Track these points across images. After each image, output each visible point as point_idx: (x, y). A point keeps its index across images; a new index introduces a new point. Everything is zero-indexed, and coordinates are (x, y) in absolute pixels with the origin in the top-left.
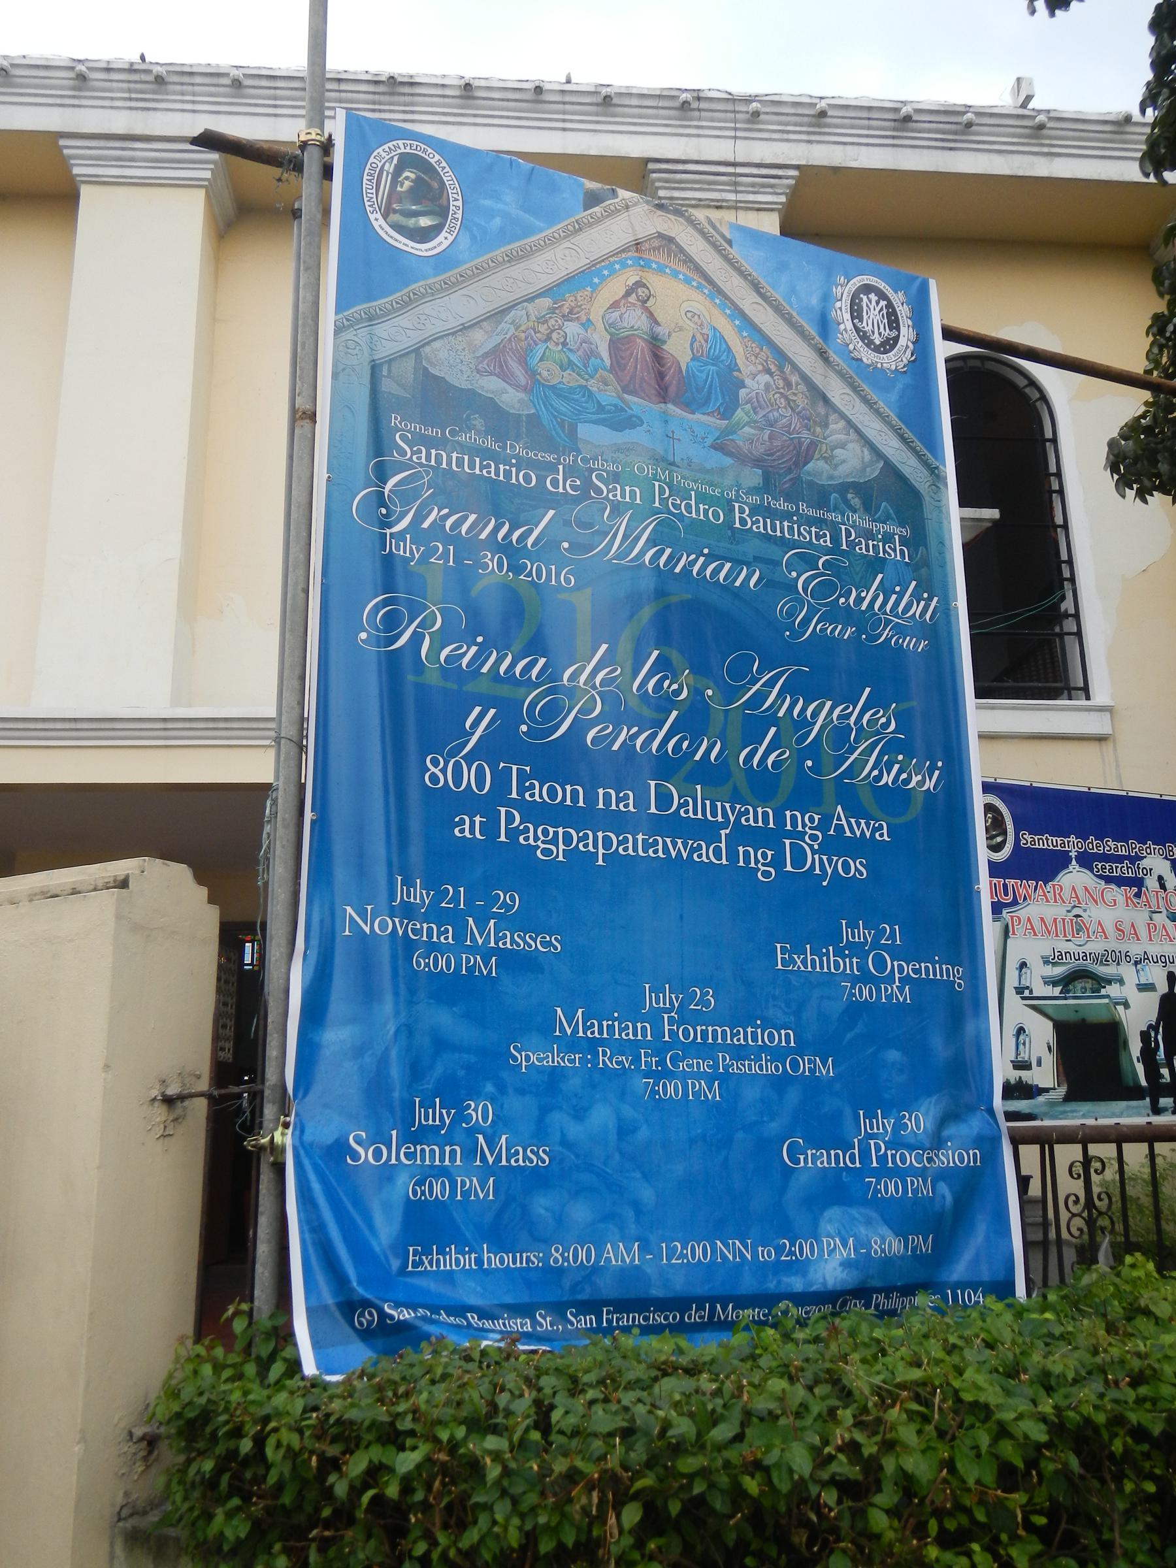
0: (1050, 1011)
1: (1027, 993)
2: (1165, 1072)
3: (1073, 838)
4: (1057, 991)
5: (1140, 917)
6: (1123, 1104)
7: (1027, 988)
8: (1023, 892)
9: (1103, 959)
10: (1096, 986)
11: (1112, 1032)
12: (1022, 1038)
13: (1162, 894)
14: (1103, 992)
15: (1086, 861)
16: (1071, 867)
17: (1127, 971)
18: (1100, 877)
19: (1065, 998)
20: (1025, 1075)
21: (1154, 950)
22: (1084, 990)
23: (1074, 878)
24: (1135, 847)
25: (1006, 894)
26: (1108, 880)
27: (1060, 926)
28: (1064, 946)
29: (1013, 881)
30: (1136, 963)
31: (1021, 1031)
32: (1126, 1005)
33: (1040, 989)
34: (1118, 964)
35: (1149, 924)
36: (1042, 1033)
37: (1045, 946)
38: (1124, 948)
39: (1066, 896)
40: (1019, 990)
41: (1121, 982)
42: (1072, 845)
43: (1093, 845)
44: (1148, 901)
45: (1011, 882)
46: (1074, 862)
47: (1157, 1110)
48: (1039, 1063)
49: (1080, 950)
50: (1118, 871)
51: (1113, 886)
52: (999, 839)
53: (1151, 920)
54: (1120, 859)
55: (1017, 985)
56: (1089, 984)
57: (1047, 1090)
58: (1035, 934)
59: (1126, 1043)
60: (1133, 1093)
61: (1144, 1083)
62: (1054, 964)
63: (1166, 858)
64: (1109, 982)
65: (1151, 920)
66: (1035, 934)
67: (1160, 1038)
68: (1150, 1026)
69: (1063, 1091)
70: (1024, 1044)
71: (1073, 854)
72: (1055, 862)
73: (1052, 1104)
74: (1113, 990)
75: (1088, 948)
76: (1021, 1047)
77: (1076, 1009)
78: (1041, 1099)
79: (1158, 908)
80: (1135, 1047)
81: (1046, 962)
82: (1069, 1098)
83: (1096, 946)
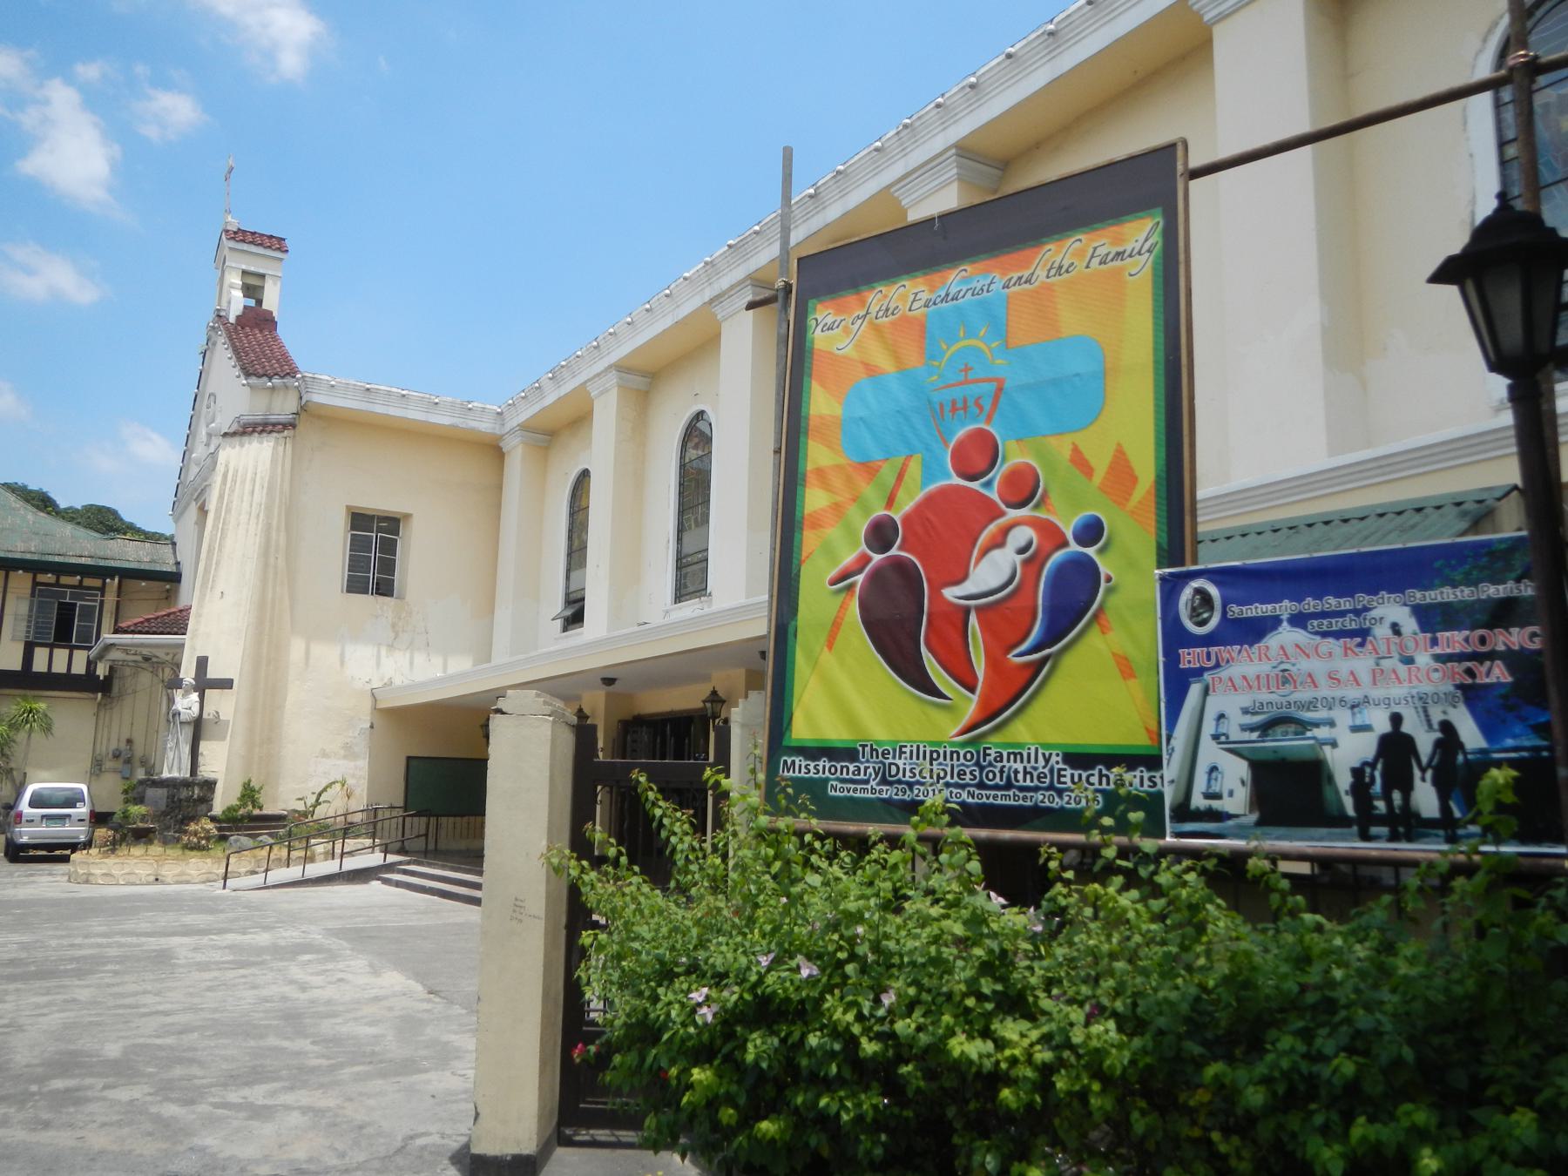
0: (1246, 753)
1: (1223, 739)
2: (1381, 805)
3: (1286, 603)
4: (1255, 736)
5: (1362, 664)
6: (1323, 831)
7: (1224, 734)
8: (1225, 656)
9: (1311, 705)
10: (1300, 729)
11: (1313, 771)
12: (1214, 775)
13: (1396, 639)
14: (1309, 734)
15: (1299, 620)
16: (1280, 629)
17: (1344, 718)
18: (1316, 633)
19: (1263, 741)
20: (1216, 804)
21: (1376, 693)
22: (1286, 733)
23: (1287, 636)
24: (1363, 599)
25: (1209, 659)
26: (1325, 635)
27: (1263, 681)
28: (1264, 696)
29: (1216, 649)
30: (1353, 707)
31: (1214, 769)
32: (1334, 744)
33: (1236, 734)
34: (1330, 709)
35: (1374, 670)
36: (1236, 772)
37: (1245, 700)
38: (1338, 693)
39: (1272, 653)
40: (1216, 737)
41: (1332, 724)
42: (1286, 608)
43: (1310, 604)
44: (1375, 649)
45: (1213, 650)
46: (1285, 624)
47: (1365, 836)
48: (1231, 794)
49: (1284, 700)
50: (1337, 624)
51: (1331, 640)
52: (1205, 615)
53: (1378, 665)
54: (1342, 614)
55: (1213, 732)
56: (1292, 728)
57: (1237, 816)
58: (1236, 690)
59: (1330, 779)
60: (1340, 820)
61: (1350, 810)
62: (1256, 713)
63: (1405, 605)
64: (1317, 725)
65: (1378, 665)
66: (1236, 690)
67: (1377, 774)
68: (1365, 764)
69: (1254, 817)
70: (1216, 779)
71: (1285, 617)
72: (1264, 627)
73: (1241, 827)
74: (1322, 733)
75: (1293, 698)
76: (1213, 782)
77: (1275, 750)
78: (1230, 823)
79: (1389, 652)
80: (1344, 781)
81: (1246, 711)
82: (1260, 823)
83: (1304, 695)
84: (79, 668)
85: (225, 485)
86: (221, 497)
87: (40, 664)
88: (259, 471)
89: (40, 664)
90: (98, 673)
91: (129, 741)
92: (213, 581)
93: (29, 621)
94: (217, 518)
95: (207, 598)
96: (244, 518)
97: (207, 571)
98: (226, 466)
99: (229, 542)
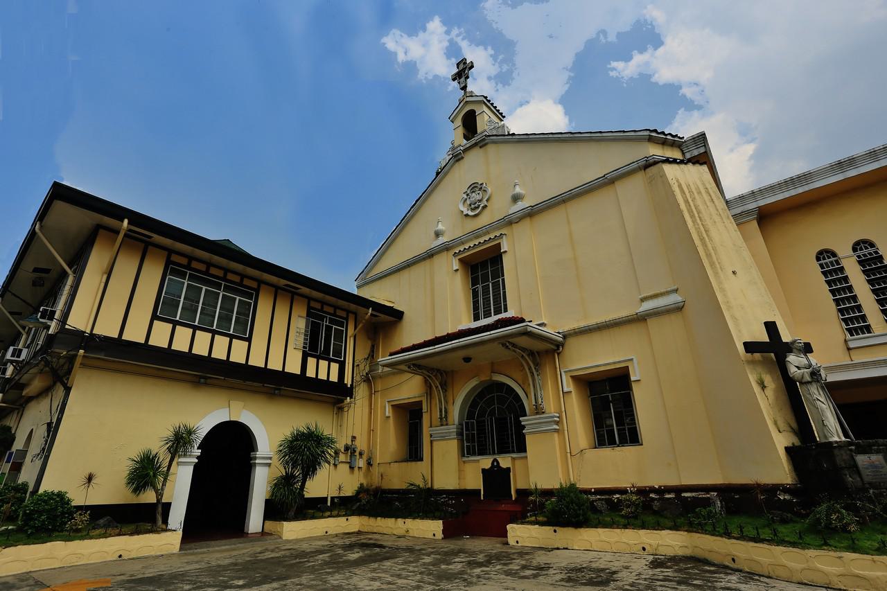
84: (334, 378)
85: (685, 194)
86: (687, 202)
87: (311, 373)
88: (709, 187)
89: (311, 373)
90: (346, 382)
91: (354, 438)
92: (719, 263)
93: (306, 335)
94: (692, 216)
95: (722, 276)
96: (717, 219)
97: (709, 255)
98: (678, 181)
99: (713, 233)
